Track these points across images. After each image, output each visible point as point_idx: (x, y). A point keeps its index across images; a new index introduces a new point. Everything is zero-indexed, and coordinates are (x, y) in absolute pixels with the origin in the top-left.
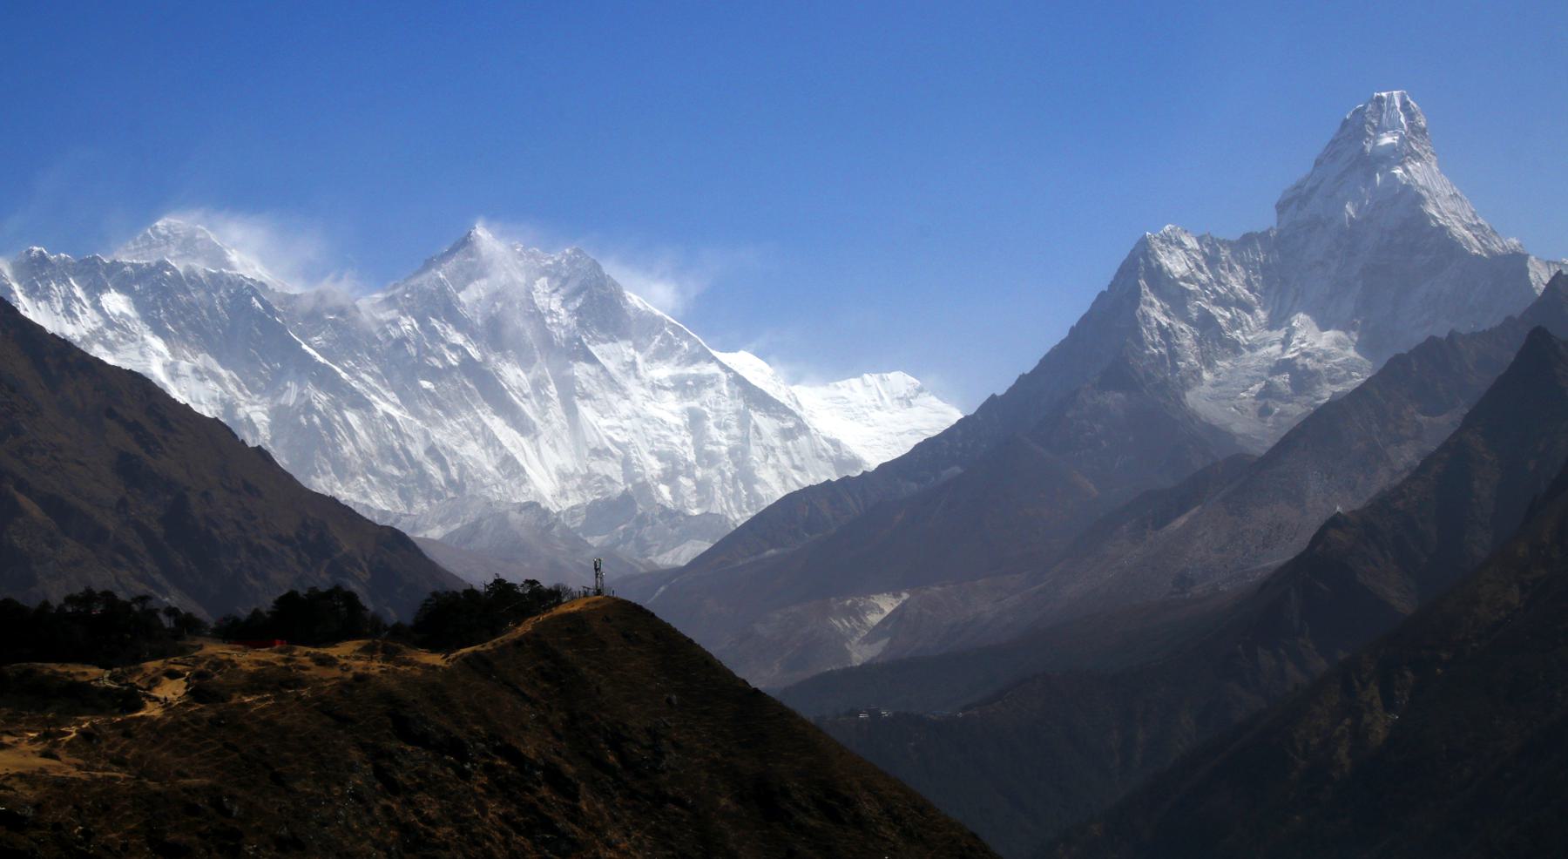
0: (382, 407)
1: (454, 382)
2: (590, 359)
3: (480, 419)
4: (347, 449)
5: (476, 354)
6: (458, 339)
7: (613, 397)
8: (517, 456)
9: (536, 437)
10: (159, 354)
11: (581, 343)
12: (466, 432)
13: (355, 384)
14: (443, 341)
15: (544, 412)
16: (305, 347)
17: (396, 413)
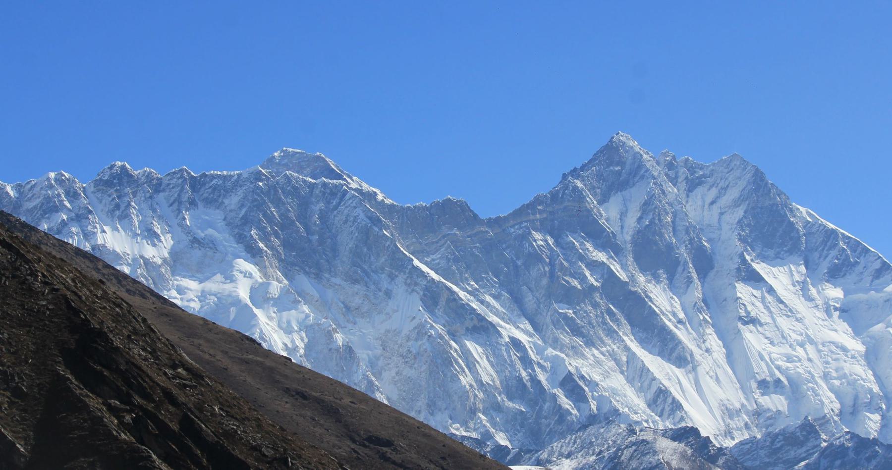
0: (508, 331)
1: (595, 305)
2: (754, 279)
3: (627, 349)
4: (466, 380)
5: (623, 276)
6: (601, 256)
7: (782, 322)
8: (672, 390)
9: (694, 369)
10: (247, 275)
11: (744, 261)
12: (612, 364)
13: (475, 305)
14: (582, 258)
15: (702, 338)
16: (416, 262)
17: (523, 338)
